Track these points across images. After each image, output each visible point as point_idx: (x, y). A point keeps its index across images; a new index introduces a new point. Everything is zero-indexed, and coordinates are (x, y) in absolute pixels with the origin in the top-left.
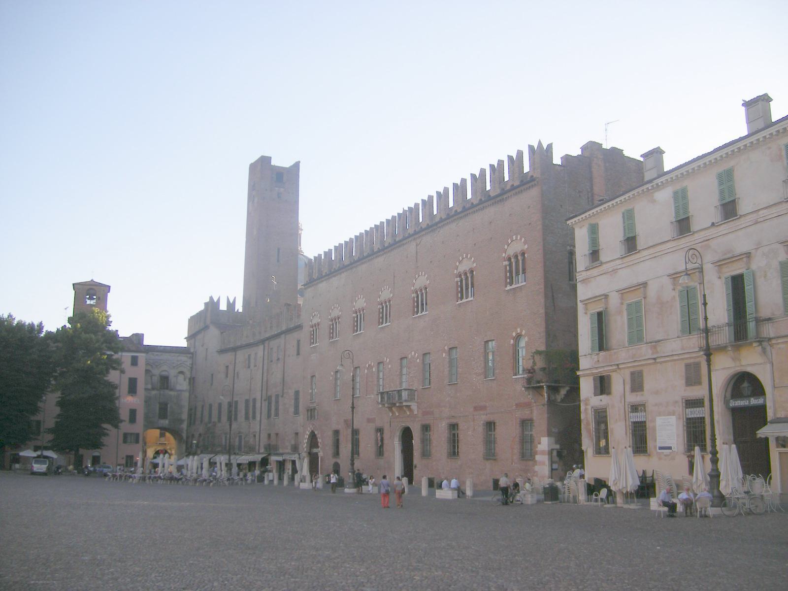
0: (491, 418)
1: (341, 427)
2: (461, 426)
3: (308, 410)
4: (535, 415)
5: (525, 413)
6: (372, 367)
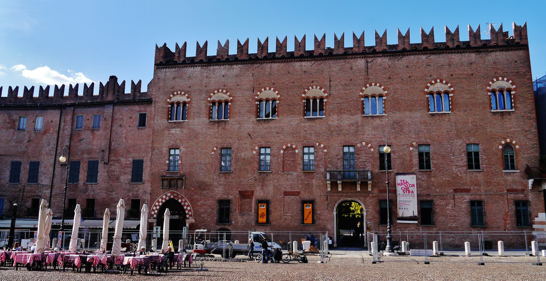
0: (478, 198)
1: (233, 196)
2: (438, 202)
3: (163, 180)
4: (531, 197)
5: (521, 196)
6: (295, 149)
